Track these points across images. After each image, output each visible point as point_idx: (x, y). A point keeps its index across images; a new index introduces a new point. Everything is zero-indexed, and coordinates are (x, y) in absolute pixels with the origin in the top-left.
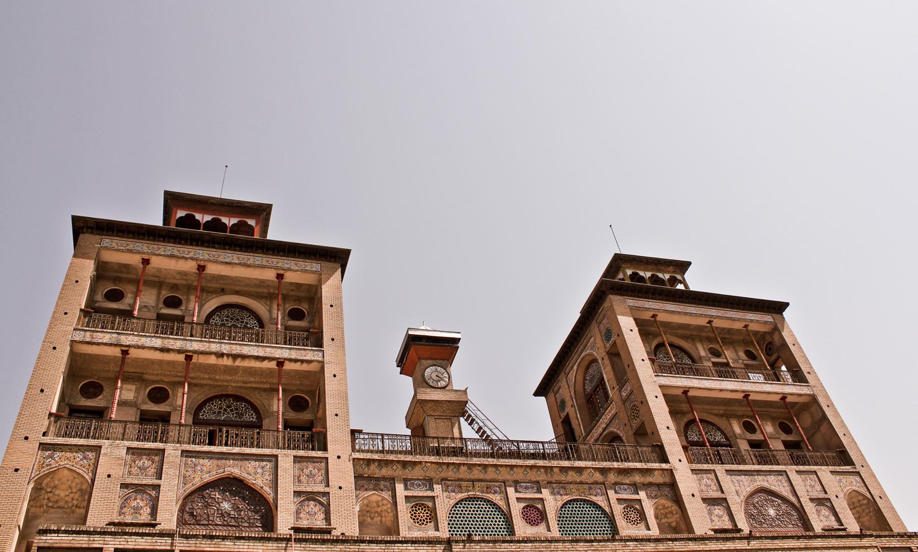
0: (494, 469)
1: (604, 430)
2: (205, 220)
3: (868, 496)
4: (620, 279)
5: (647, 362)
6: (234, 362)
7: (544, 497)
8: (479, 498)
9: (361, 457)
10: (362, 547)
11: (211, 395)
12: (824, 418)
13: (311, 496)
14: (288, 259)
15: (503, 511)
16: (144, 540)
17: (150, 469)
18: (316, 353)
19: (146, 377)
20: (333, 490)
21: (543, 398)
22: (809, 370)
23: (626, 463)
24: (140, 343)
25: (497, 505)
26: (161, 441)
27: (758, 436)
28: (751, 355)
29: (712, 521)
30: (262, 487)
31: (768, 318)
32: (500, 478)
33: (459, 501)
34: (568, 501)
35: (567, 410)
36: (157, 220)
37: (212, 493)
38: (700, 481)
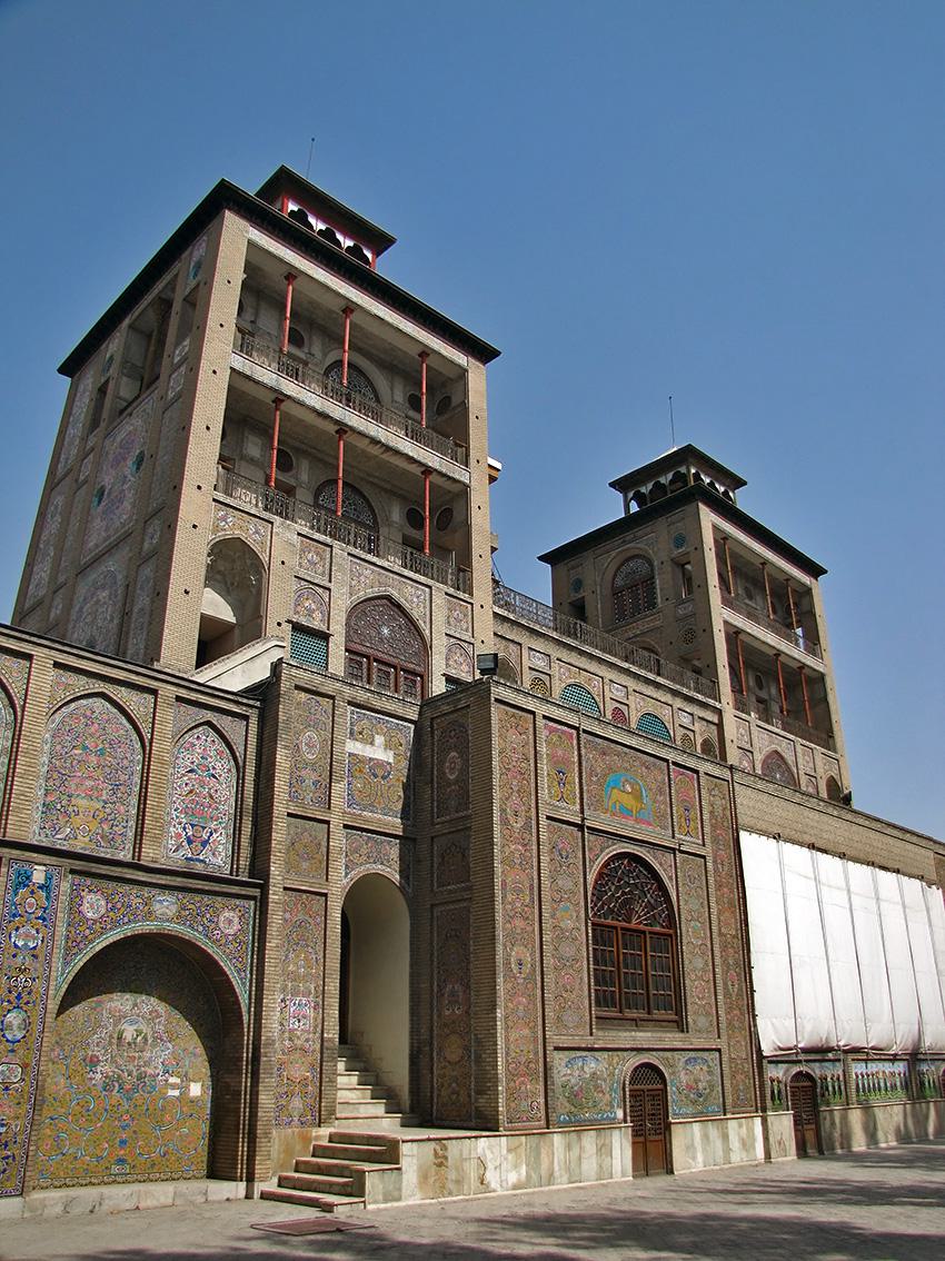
1: (636, 636)
27: (764, 695)
31: (806, 579)
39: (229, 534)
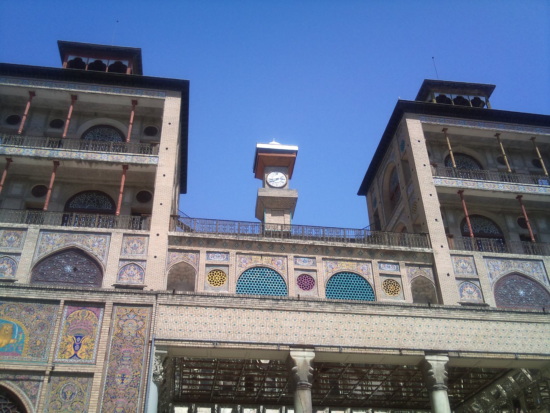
0: (279, 246)
1: (397, 221)
2: (110, 64)
5: (429, 167)
6: (91, 166)
7: (318, 269)
8: (264, 267)
9: (175, 235)
10: (85, 296)
11: (80, 191)
13: (133, 262)
14: (140, 88)
15: (282, 278)
17: (15, 242)
18: (153, 158)
20: (150, 260)
23: (392, 247)
24: (18, 153)
25: (279, 273)
26: (27, 223)
29: (462, 296)
30: (96, 256)
32: (284, 254)
33: (248, 269)
34: (337, 273)
35: (377, 205)
37: (60, 259)
38: (458, 264)
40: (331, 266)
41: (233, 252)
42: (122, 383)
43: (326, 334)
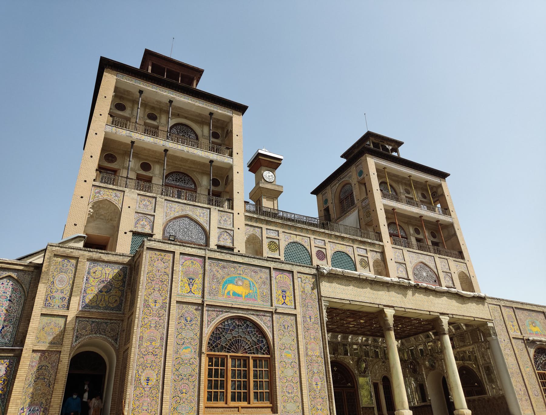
3: (468, 275)
4: (367, 144)
5: (379, 191)
8: (298, 243)
12: (455, 234)
15: (308, 251)
16: (192, 251)
18: (230, 159)
19: (140, 156)
20: (236, 230)
21: (315, 196)
22: (452, 210)
27: (420, 236)
28: (424, 196)
29: (398, 273)
32: (308, 236)
36: (137, 64)
39: (101, 198)
40: (333, 247)
41: (281, 230)
42: (310, 321)
43: (398, 301)
